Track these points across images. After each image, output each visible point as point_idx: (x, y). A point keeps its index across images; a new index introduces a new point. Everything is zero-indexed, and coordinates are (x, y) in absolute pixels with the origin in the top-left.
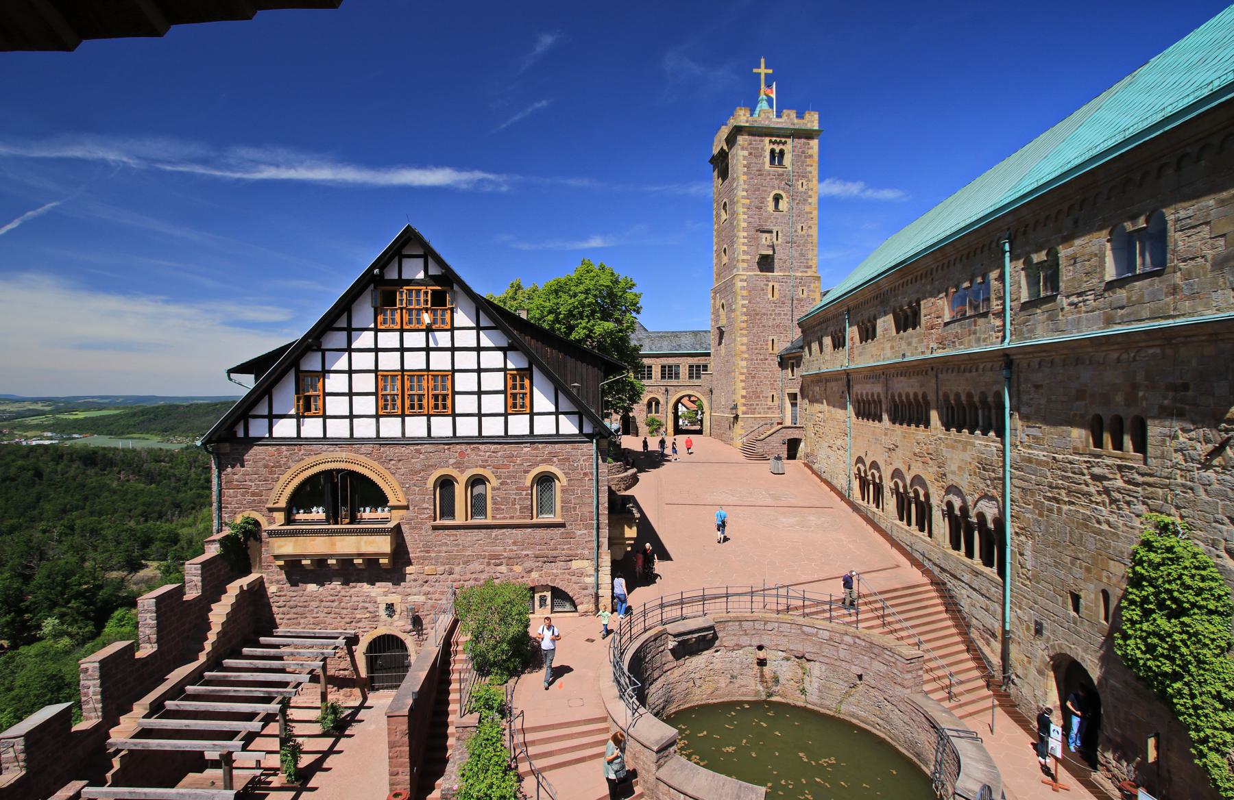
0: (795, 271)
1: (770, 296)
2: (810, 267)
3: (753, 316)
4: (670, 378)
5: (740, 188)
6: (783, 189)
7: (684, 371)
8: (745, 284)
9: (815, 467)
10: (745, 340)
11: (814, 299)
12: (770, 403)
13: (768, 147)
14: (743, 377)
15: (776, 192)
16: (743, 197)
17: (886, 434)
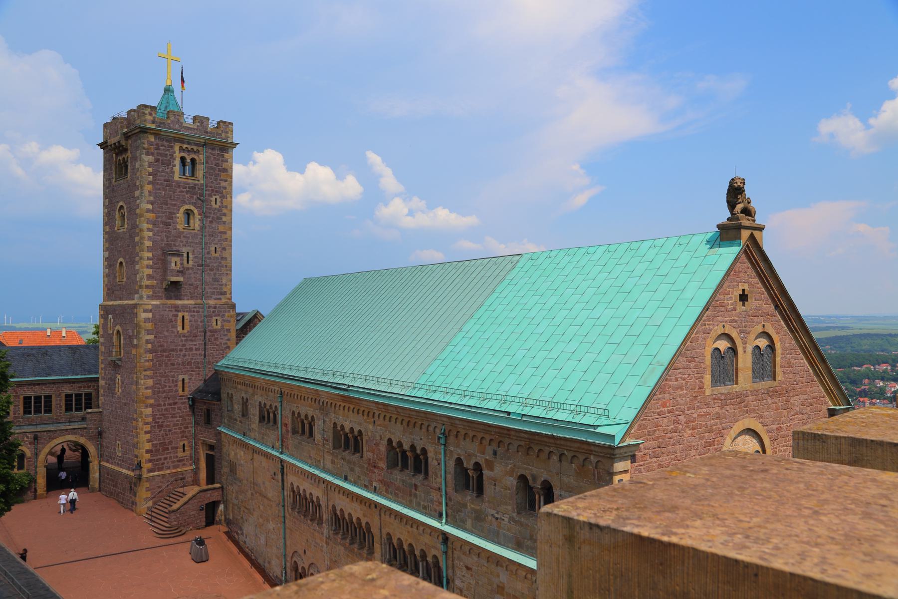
0: (208, 298)
1: (180, 328)
3: (160, 351)
4: (38, 411)
5: (144, 200)
6: (195, 205)
7: (58, 403)
8: (150, 315)
9: (241, 539)
10: (150, 382)
11: (228, 331)
12: (180, 454)
13: (178, 155)
14: (148, 428)
15: (186, 207)
16: (148, 211)
17: (328, 544)
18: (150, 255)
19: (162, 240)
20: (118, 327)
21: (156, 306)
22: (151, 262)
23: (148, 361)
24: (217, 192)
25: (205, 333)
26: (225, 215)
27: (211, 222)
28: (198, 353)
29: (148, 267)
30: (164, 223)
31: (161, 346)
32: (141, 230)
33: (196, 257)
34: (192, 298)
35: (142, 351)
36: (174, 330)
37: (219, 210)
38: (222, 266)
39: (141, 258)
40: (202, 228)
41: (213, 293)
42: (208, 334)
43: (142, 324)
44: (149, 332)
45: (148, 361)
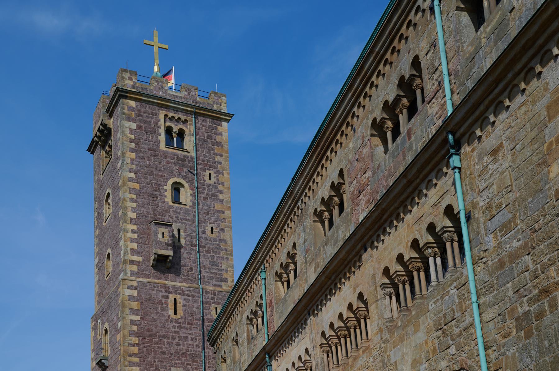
1: (171, 312)
2: (226, 280)
6: (185, 178)
8: (135, 293)
18: (135, 227)
19: (148, 213)
20: (106, 325)
21: (143, 283)
22: (135, 236)
23: (134, 345)
24: (210, 166)
25: (203, 321)
26: (221, 192)
27: (205, 198)
28: (195, 343)
29: (132, 240)
30: (150, 195)
31: (149, 330)
32: (124, 200)
33: (188, 236)
34: (185, 281)
35: (126, 333)
36: (165, 313)
37: (214, 187)
38: (221, 249)
39: (125, 230)
40: (194, 204)
41: (211, 279)
42: (206, 323)
43: (127, 302)
44: (133, 312)
45: (134, 345)
